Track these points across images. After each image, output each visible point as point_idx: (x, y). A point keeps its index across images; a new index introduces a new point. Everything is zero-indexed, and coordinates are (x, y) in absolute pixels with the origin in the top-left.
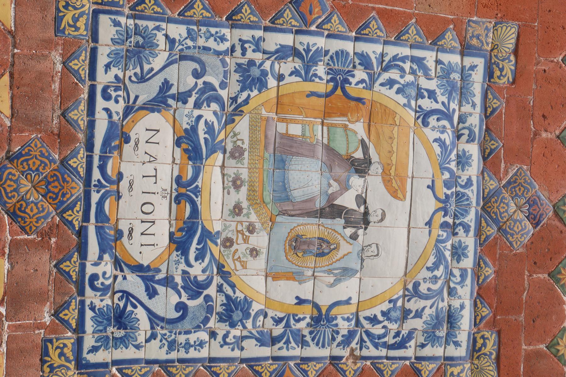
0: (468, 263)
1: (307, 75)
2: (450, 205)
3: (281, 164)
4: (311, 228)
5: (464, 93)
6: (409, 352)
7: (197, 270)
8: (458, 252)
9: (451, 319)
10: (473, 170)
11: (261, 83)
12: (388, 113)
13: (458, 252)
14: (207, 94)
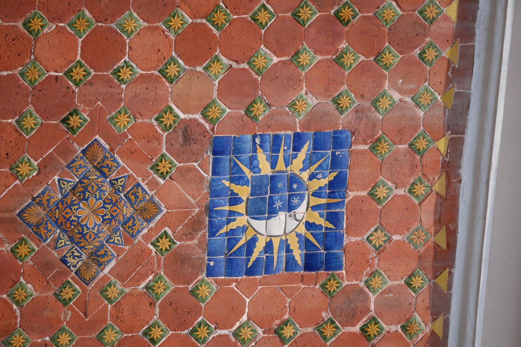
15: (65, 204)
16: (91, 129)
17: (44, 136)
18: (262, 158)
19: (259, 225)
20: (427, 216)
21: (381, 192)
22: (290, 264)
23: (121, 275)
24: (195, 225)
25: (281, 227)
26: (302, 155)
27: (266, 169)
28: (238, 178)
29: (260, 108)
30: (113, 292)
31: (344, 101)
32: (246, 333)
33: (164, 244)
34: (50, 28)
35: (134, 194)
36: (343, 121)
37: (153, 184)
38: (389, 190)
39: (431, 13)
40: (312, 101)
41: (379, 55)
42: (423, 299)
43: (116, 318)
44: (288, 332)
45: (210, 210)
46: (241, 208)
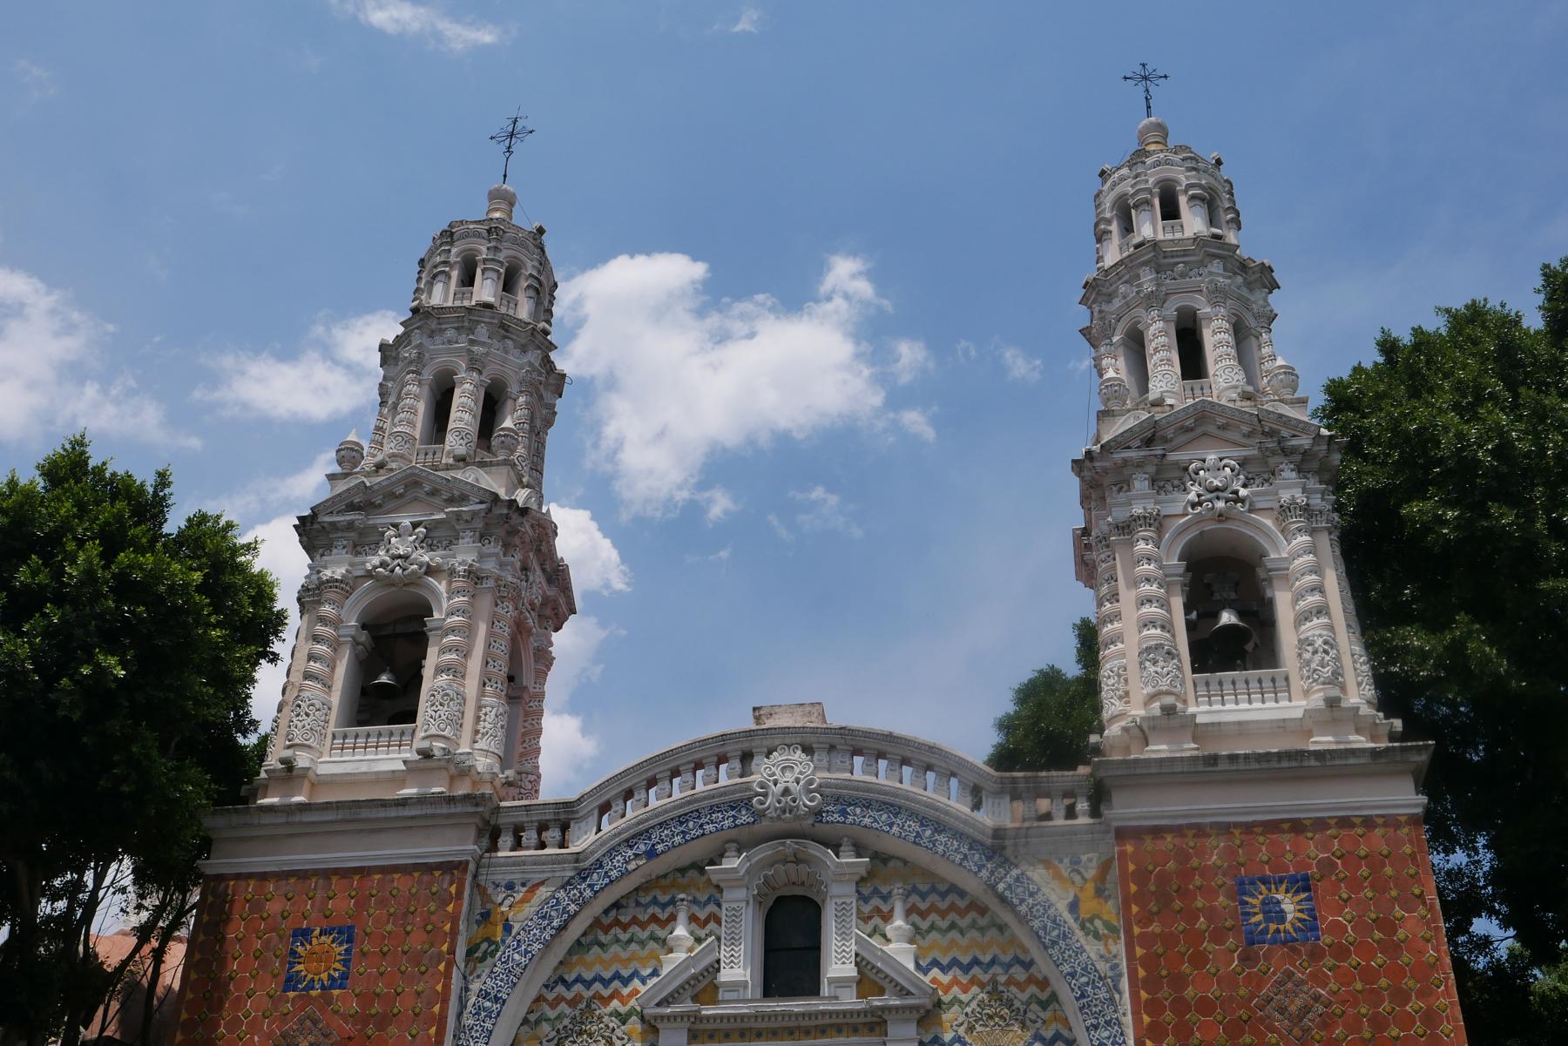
16: (1249, 1008)
18: (1253, 920)
19: (1290, 917)
21: (1265, 858)
22: (1309, 899)
23: (1324, 985)
24: (1293, 949)
25: (1289, 906)
28: (1266, 931)
29: (1229, 923)
30: (1335, 988)
32: (1348, 917)
34: (1198, 1035)
35: (1280, 983)
37: (1274, 973)
38: (1264, 855)
40: (1221, 898)
43: (1349, 985)
44: (1345, 896)
45: (1284, 943)
46: (1281, 927)
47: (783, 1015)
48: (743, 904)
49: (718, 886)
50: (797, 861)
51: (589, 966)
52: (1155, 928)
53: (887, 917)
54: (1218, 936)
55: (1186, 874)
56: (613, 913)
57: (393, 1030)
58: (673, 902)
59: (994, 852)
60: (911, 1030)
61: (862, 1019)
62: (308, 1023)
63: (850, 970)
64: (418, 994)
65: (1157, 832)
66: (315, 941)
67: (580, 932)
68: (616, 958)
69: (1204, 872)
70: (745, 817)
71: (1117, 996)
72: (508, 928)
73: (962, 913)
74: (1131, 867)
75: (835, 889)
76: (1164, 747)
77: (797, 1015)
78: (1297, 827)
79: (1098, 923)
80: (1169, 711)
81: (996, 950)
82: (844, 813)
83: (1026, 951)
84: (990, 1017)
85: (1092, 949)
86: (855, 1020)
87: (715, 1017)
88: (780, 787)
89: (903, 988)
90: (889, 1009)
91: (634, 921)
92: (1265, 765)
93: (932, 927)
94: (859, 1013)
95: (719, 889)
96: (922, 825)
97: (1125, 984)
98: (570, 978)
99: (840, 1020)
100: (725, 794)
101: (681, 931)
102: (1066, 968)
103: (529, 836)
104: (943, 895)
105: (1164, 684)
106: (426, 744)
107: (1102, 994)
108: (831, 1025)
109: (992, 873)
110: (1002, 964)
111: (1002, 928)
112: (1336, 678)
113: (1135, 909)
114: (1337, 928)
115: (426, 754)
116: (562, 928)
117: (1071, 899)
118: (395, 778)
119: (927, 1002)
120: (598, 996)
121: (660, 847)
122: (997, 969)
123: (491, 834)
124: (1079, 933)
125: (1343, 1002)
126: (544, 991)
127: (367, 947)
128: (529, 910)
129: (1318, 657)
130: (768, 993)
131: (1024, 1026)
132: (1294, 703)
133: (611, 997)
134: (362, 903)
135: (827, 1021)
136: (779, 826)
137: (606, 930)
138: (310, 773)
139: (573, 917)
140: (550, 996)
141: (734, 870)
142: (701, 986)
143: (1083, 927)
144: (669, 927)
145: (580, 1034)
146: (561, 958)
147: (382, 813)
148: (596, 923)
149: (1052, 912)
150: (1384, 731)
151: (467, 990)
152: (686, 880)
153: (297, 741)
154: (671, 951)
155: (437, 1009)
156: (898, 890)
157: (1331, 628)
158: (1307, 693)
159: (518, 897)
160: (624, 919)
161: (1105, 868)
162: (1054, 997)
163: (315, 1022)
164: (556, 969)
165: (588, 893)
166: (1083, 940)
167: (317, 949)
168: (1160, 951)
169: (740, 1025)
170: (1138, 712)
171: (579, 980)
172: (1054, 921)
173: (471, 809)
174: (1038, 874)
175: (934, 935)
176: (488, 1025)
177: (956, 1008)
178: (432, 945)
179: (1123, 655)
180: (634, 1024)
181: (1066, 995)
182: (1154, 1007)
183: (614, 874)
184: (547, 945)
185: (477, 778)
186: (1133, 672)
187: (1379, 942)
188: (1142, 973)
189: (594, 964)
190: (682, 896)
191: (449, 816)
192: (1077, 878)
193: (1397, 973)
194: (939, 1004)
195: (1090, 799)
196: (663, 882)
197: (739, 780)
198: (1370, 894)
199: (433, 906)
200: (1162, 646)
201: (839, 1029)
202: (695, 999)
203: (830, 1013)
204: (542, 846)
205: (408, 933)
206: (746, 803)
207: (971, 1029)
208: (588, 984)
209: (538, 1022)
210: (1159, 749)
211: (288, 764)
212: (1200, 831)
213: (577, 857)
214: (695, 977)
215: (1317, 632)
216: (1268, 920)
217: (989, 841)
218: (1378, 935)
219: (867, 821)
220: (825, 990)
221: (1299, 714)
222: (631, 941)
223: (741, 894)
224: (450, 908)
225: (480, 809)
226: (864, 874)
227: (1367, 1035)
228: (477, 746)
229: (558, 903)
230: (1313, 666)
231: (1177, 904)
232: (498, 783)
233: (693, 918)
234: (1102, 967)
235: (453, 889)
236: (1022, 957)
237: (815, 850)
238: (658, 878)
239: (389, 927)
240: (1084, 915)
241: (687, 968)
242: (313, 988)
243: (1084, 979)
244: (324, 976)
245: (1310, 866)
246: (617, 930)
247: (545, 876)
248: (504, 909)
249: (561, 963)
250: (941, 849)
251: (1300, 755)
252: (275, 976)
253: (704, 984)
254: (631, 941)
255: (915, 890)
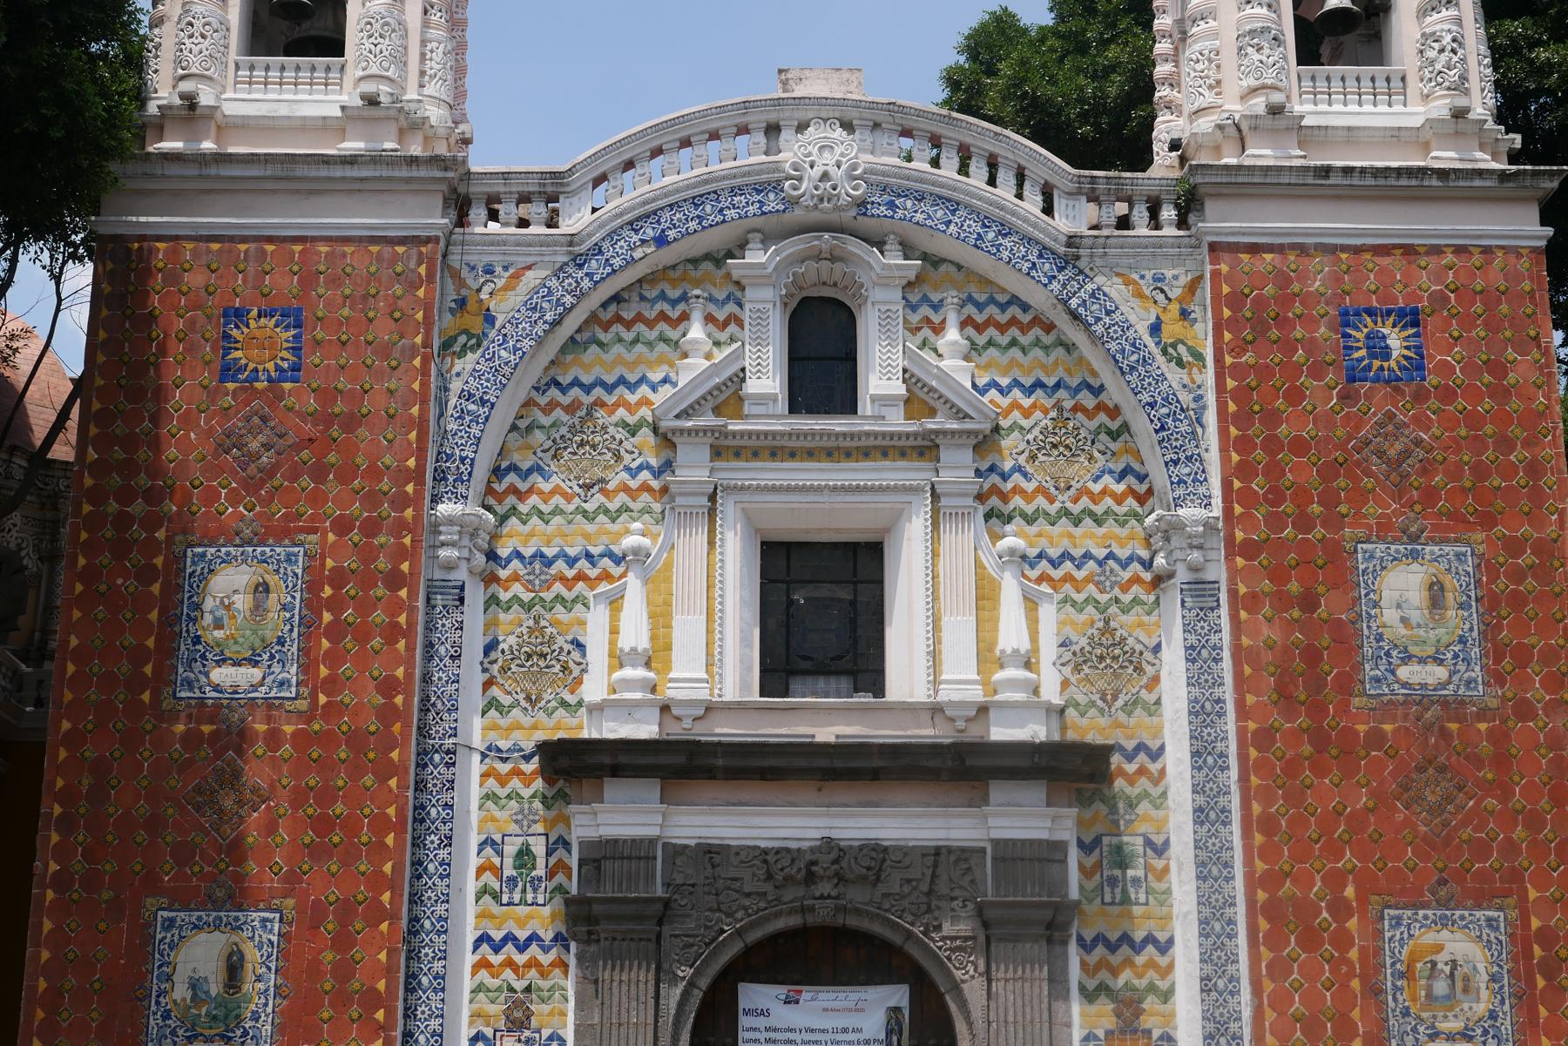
0: (1466, 913)
1: (1402, 989)
2: (1445, 923)
3: (1437, 998)
4: (1459, 985)
5: (1399, 920)
6: (1503, 938)
7: (1479, 1032)
8: (1462, 918)
9: (1489, 920)
10: (1430, 913)
11: (1408, 1008)
12: (1412, 953)
13: (1462, 918)
14: (1415, 1030)
15: (1388, 462)
16: (1345, 450)
17: (1350, 476)
19: (1395, 354)
20: (1385, 261)
21: (1373, 287)
23: (1427, 430)
24: (1397, 390)
26: (1353, 333)
27: (1363, 352)
28: (1369, 367)
30: (1438, 433)
31: (1322, 312)
32: (1458, 357)
33: (1409, 406)
35: (1380, 424)
36: (1333, 312)
37: (1374, 414)
38: (1371, 283)
39: (1270, 268)
40: (1323, 330)
41: (1295, 295)
42: (1433, 259)
44: (1456, 334)
45: (1388, 382)
46: (1386, 365)
47: (822, 434)
48: (770, 306)
49: (738, 283)
50: (833, 259)
51: (587, 368)
52: (1248, 358)
53: (939, 329)
54: (1317, 372)
55: (1287, 300)
56: (613, 308)
57: (362, 432)
58: (684, 298)
59: (1067, 262)
60: (967, 456)
61: (911, 442)
62: (256, 420)
63: (899, 389)
64: (390, 392)
65: (1254, 249)
66: (252, 323)
67: (576, 327)
68: (620, 360)
69: (1306, 299)
70: (773, 203)
71: (1199, 430)
72: (490, 320)
73: (1024, 329)
74: (1226, 289)
75: (877, 294)
76: (1268, 152)
77: (837, 435)
78: (1409, 251)
79: (1181, 349)
80: (1275, 111)
81: (1061, 372)
82: (891, 205)
83: (1094, 374)
84: (1055, 446)
85: (1175, 376)
86: (903, 443)
87: (742, 434)
88: (817, 172)
89: (959, 410)
90: (944, 433)
91: (639, 318)
92: (1381, 182)
93: (990, 343)
94: (908, 435)
95: (743, 289)
96: (984, 226)
97: (1211, 418)
98: (565, 380)
99: (887, 443)
100: (748, 174)
101: (696, 331)
102: (1146, 397)
103: (507, 209)
104: (1003, 307)
105: (1269, 77)
106: (369, 87)
107: (1184, 427)
108: (875, 447)
109: (1064, 286)
110: (1067, 388)
111: (1069, 348)
112: (1461, 86)
113: (1227, 336)
114: (1445, 368)
115: (372, 101)
116: (556, 323)
117: (1153, 319)
118: (323, 126)
119: (986, 427)
120: (600, 403)
121: (671, 234)
122: (1062, 394)
123: (460, 206)
124: (1160, 359)
125: (1446, 449)
126: (534, 394)
127: (319, 334)
128: (515, 299)
129: (1444, 57)
130: (794, 409)
131: (1091, 458)
132: (1409, 109)
133: (617, 405)
134: (308, 280)
135: (871, 442)
136: (816, 217)
137: (606, 327)
138: (218, 115)
139: (568, 310)
140: (543, 400)
141: (762, 266)
142: (722, 398)
143: (1165, 352)
144: (681, 328)
145: (582, 444)
146: (552, 356)
147: (324, 172)
148: (593, 318)
149: (1130, 334)
150: (1504, 148)
151: (446, 390)
152: (698, 274)
153: (194, 70)
154: (685, 355)
155: (415, 410)
156: (952, 297)
157: (1459, 21)
158: (1426, 97)
159: (500, 283)
160: (627, 315)
161: (1193, 286)
162: (1125, 427)
163: (264, 419)
164: (546, 369)
165: (586, 283)
166: (1164, 368)
167: (257, 333)
168: (1253, 384)
169: (769, 442)
170: (1235, 107)
171: (576, 382)
172: (1133, 345)
173: (439, 174)
174: (1115, 289)
175: (992, 350)
176: (475, 430)
177: (1016, 434)
178: (402, 337)
179: (1215, 35)
180: (646, 437)
181: (1142, 426)
182: (1244, 444)
183: (617, 262)
184: (540, 342)
185: (430, 133)
186: (1229, 57)
187: (1488, 386)
188: (1232, 407)
189: (591, 366)
190: (697, 292)
191: (408, 180)
192: (1160, 297)
193: (1503, 419)
194: (996, 429)
195: (1177, 206)
196: (672, 274)
197: (764, 158)
198: (1482, 334)
199: (398, 289)
200: (1269, 29)
201: (885, 453)
202: (717, 411)
203: (876, 435)
204: (524, 223)
205: (371, 320)
206: (777, 186)
207: (1033, 458)
208: (588, 389)
209: (529, 429)
210: (1261, 154)
211: (190, 101)
212: (1302, 250)
213: (572, 240)
214: (717, 387)
215: (1446, 27)
216: (1373, 356)
217: (1062, 250)
218: (1487, 378)
219: (919, 217)
220: (865, 406)
221: (1417, 122)
222: (636, 341)
223: (768, 293)
224: (421, 293)
225: (450, 174)
226: (913, 278)
227: (1468, 484)
228: (426, 91)
229: (550, 293)
230: (1438, 67)
231: (1274, 333)
232: (452, 140)
233: (709, 319)
234: (1185, 398)
235: (422, 270)
236: (1091, 380)
237: (855, 247)
238: (665, 268)
239: (346, 312)
240: (1167, 338)
241: (710, 377)
242: (257, 380)
243: (1165, 411)
244: (270, 366)
245: (1421, 299)
246: (618, 328)
247: (531, 260)
248: (484, 296)
249: (553, 362)
250: (1005, 255)
251: (1422, 172)
252: (208, 363)
253: (728, 395)
254: (636, 341)
255: (970, 299)
